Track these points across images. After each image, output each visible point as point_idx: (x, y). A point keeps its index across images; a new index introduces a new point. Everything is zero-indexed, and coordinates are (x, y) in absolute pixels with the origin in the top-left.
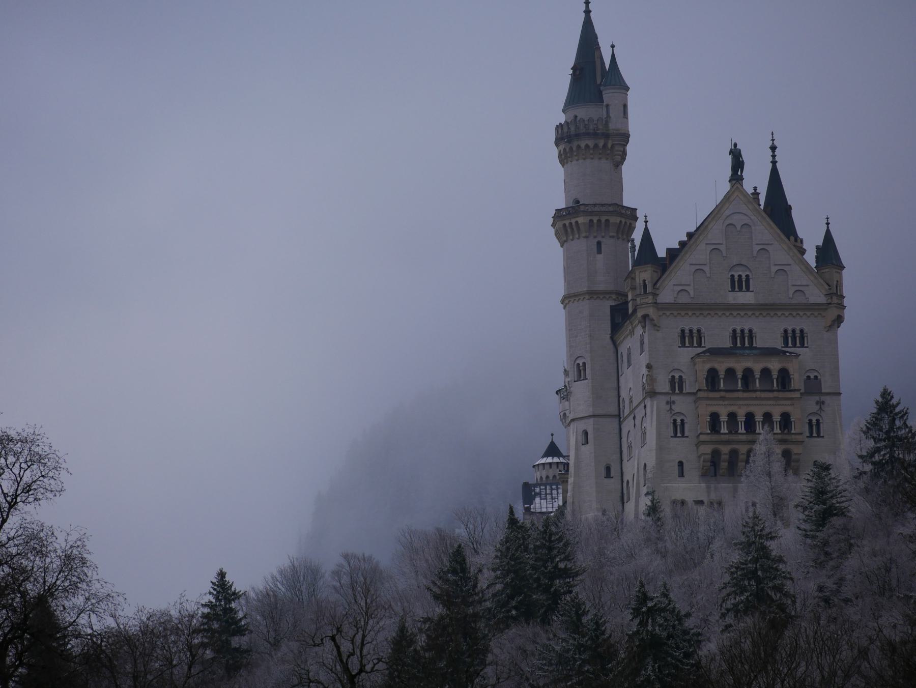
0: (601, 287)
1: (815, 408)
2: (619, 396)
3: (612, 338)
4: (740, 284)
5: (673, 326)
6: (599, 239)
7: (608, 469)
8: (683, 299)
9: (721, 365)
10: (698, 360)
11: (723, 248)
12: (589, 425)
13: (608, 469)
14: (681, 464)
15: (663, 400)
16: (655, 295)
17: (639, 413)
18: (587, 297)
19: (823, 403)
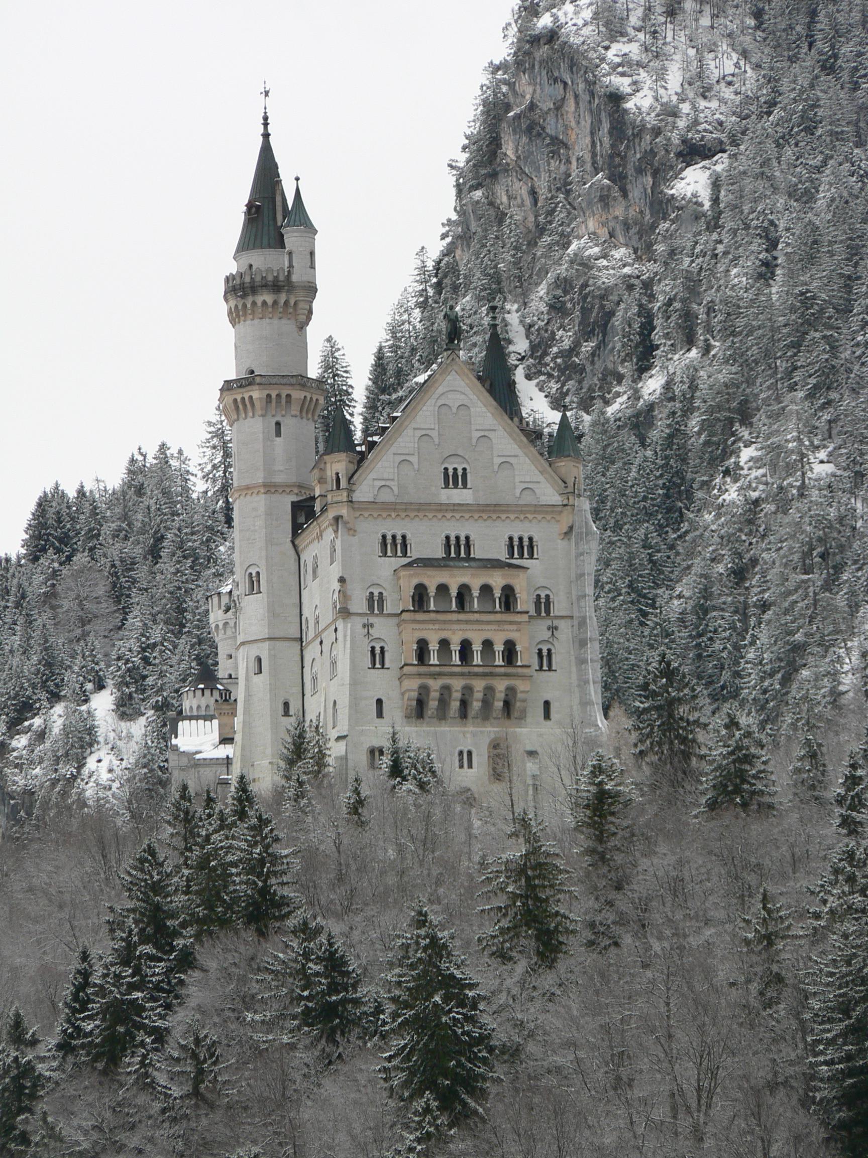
0: (279, 479)
2: (301, 615)
3: (293, 542)
5: (372, 530)
6: (278, 418)
7: (286, 705)
8: (386, 497)
10: (402, 573)
12: (263, 651)
13: (286, 705)
15: (359, 622)
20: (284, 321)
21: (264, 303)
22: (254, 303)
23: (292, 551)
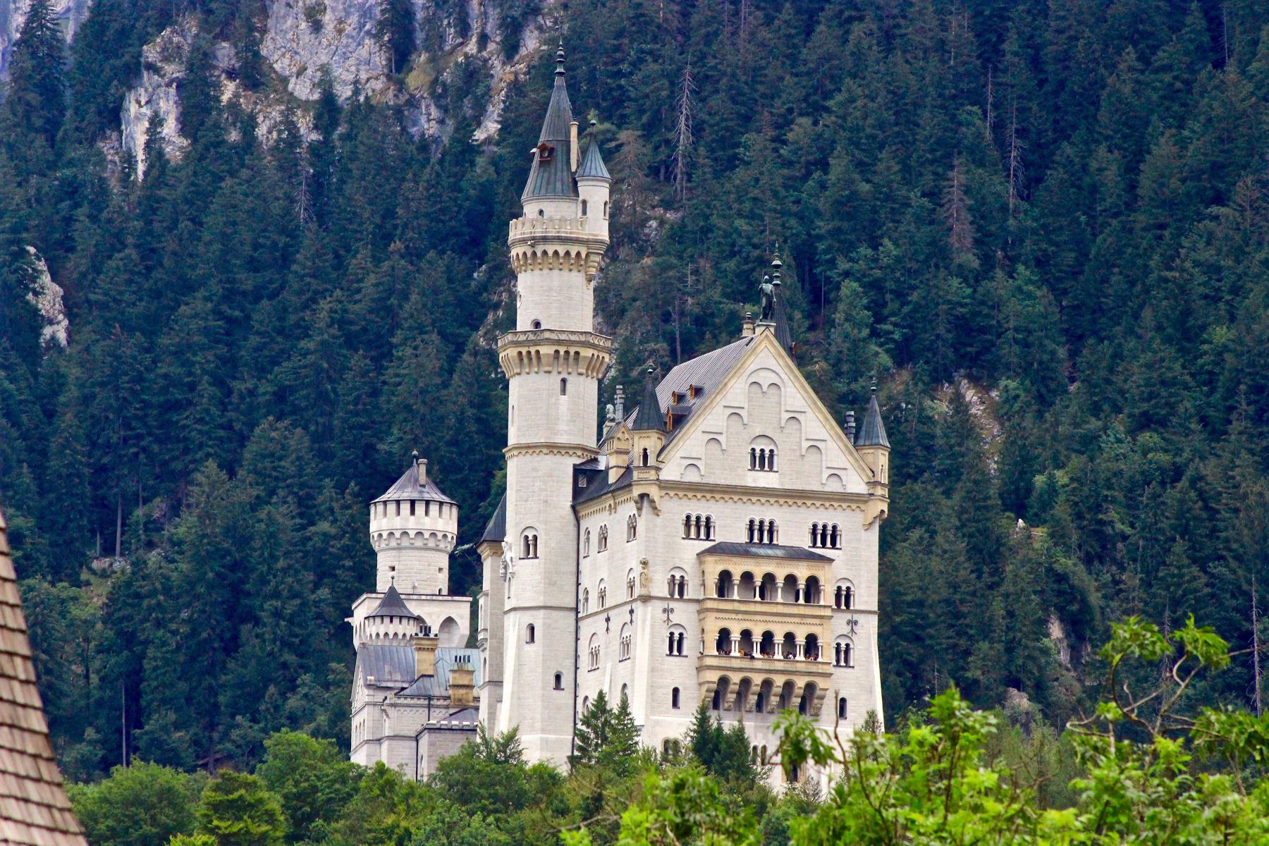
0: (562, 439)
1: (846, 629)
2: (578, 584)
3: (573, 507)
4: (762, 461)
5: (676, 509)
6: (564, 375)
7: (558, 677)
8: (692, 477)
9: (737, 568)
10: (710, 559)
11: (743, 413)
12: (538, 619)
13: (558, 677)
14: (676, 691)
15: (661, 605)
16: (658, 469)
17: (619, 617)
18: (545, 451)
19: (856, 623)
20: (575, 273)
21: (556, 253)
22: (545, 253)
23: (572, 517)
